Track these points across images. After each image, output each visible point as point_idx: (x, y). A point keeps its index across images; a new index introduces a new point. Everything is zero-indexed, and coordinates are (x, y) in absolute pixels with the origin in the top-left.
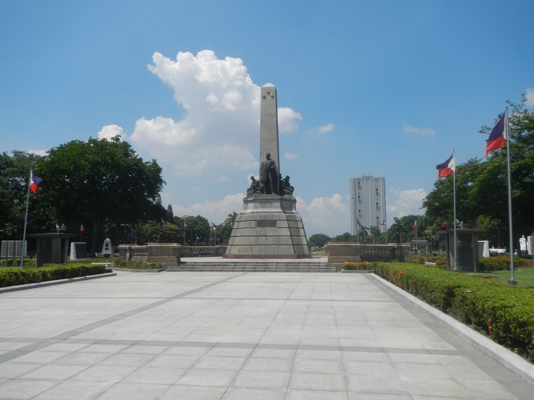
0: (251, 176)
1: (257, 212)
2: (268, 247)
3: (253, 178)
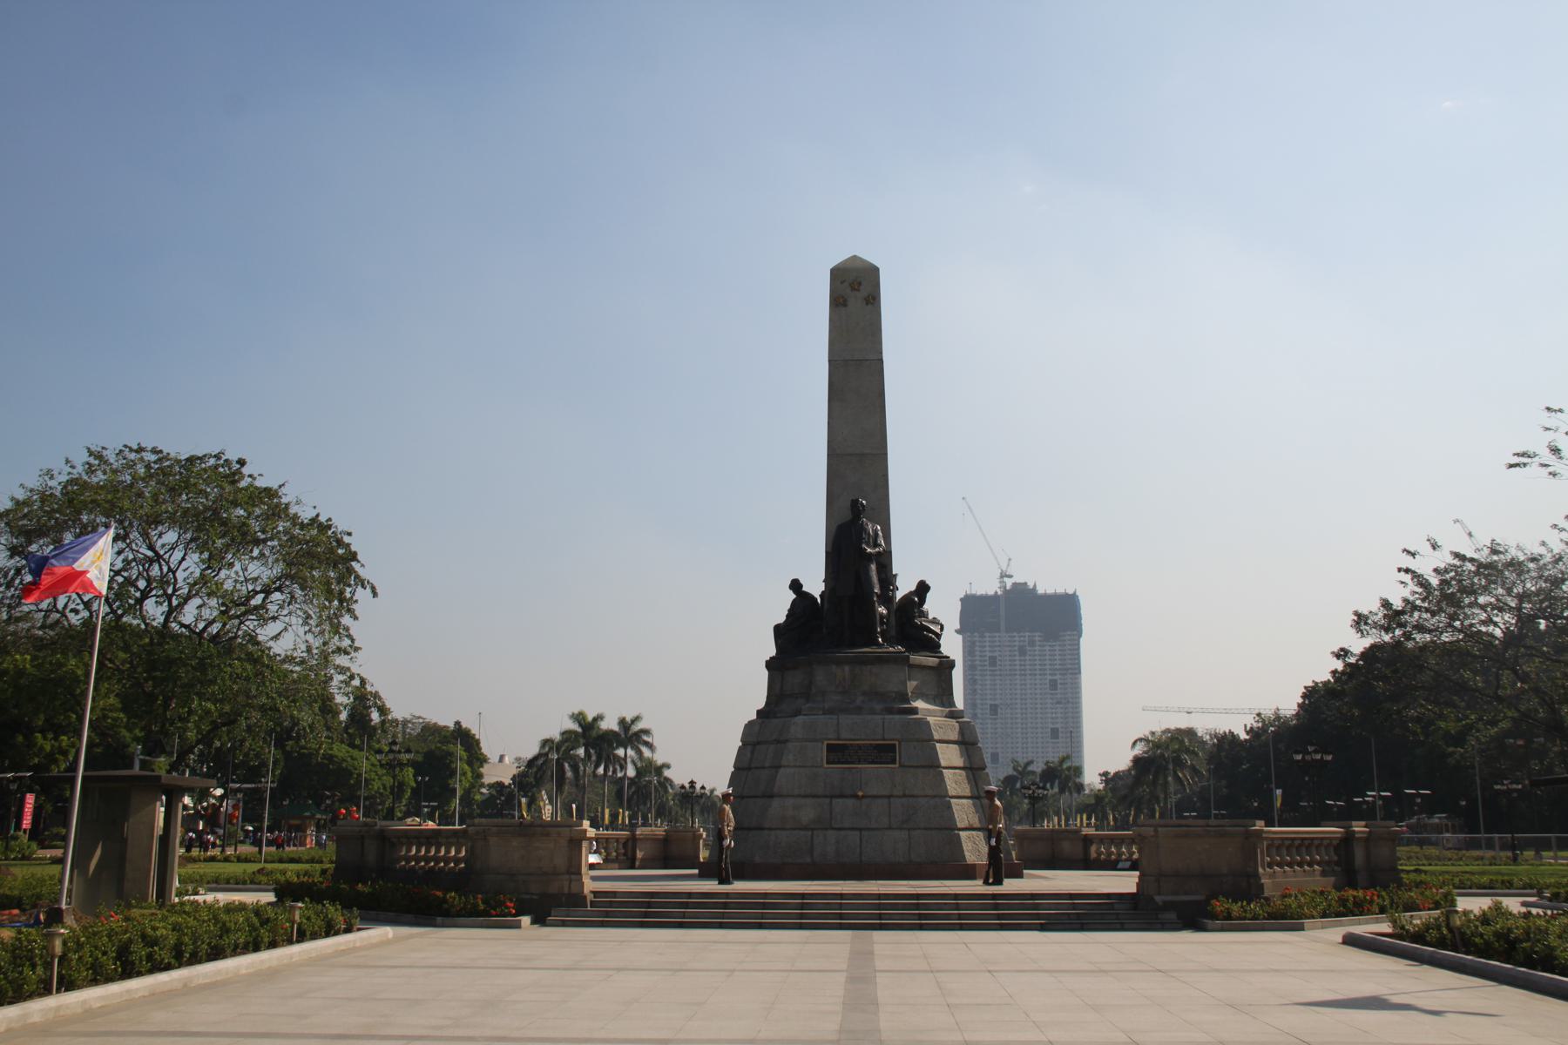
3: (796, 586)
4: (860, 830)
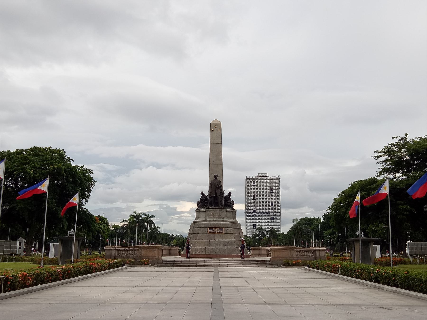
0: (201, 192)
1: (209, 221)
2: (218, 248)
3: (202, 193)
4: (216, 247)
